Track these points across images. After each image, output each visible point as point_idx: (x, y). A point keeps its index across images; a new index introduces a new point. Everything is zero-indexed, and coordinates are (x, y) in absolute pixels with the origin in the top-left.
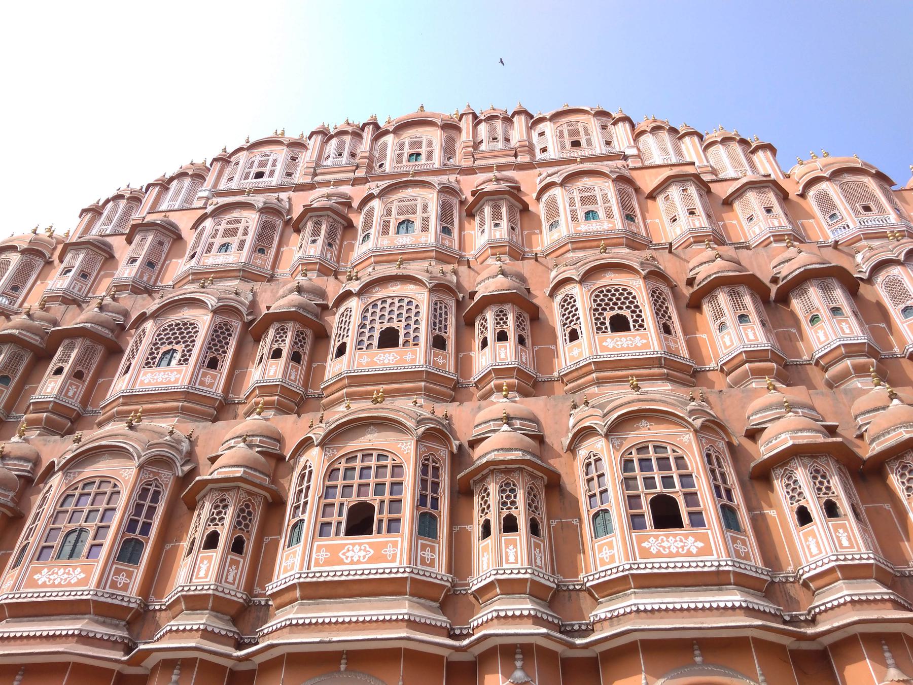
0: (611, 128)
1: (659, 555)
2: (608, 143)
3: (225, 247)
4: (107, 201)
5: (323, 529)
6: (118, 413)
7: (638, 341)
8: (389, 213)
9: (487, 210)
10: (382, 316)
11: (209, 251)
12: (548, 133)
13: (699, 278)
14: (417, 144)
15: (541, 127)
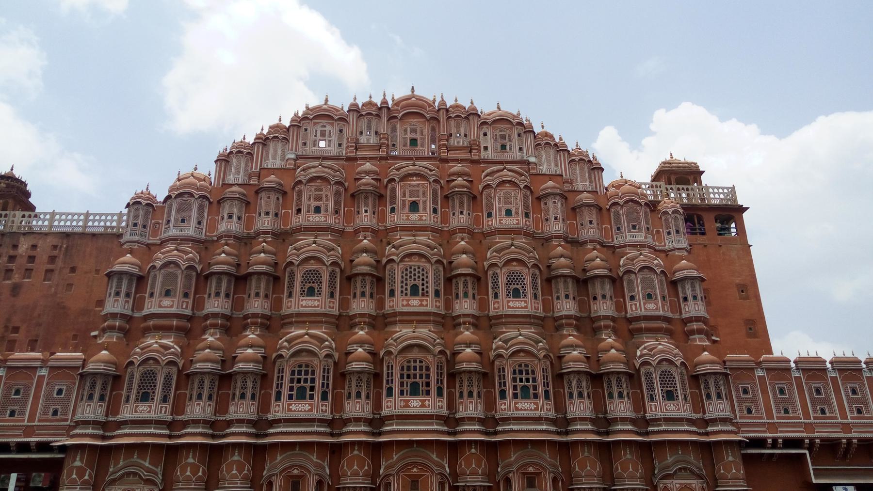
0: (523, 135)
1: (521, 410)
2: (521, 149)
3: (318, 210)
4: (231, 153)
5: (402, 393)
6: (296, 322)
7: (523, 304)
8: (404, 195)
9: (457, 202)
10: (411, 277)
11: (309, 211)
12: (488, 134)
13: (553, 266)
14: (414, 131)
15: (485, 129)
